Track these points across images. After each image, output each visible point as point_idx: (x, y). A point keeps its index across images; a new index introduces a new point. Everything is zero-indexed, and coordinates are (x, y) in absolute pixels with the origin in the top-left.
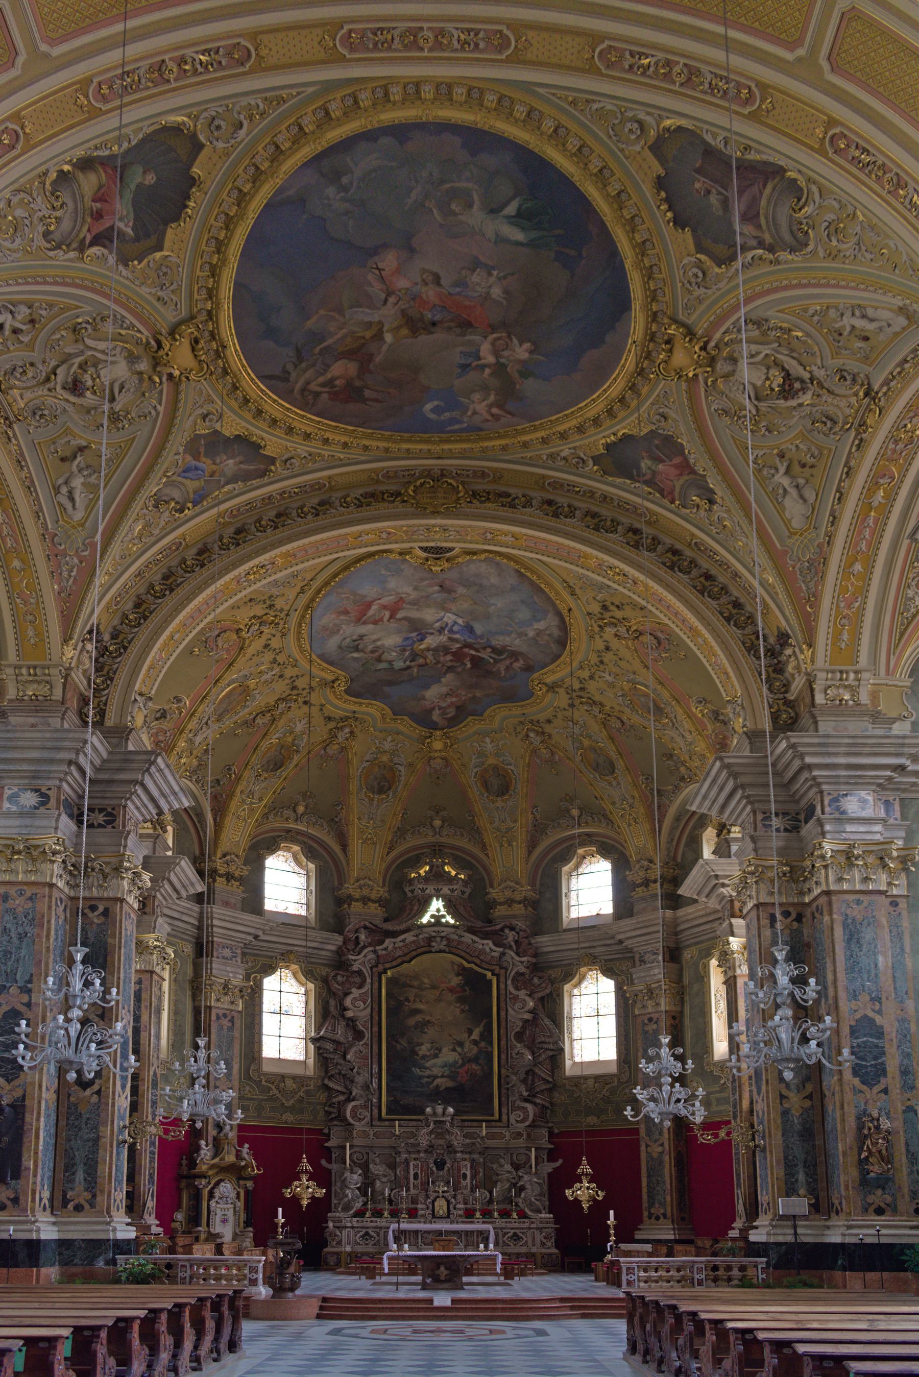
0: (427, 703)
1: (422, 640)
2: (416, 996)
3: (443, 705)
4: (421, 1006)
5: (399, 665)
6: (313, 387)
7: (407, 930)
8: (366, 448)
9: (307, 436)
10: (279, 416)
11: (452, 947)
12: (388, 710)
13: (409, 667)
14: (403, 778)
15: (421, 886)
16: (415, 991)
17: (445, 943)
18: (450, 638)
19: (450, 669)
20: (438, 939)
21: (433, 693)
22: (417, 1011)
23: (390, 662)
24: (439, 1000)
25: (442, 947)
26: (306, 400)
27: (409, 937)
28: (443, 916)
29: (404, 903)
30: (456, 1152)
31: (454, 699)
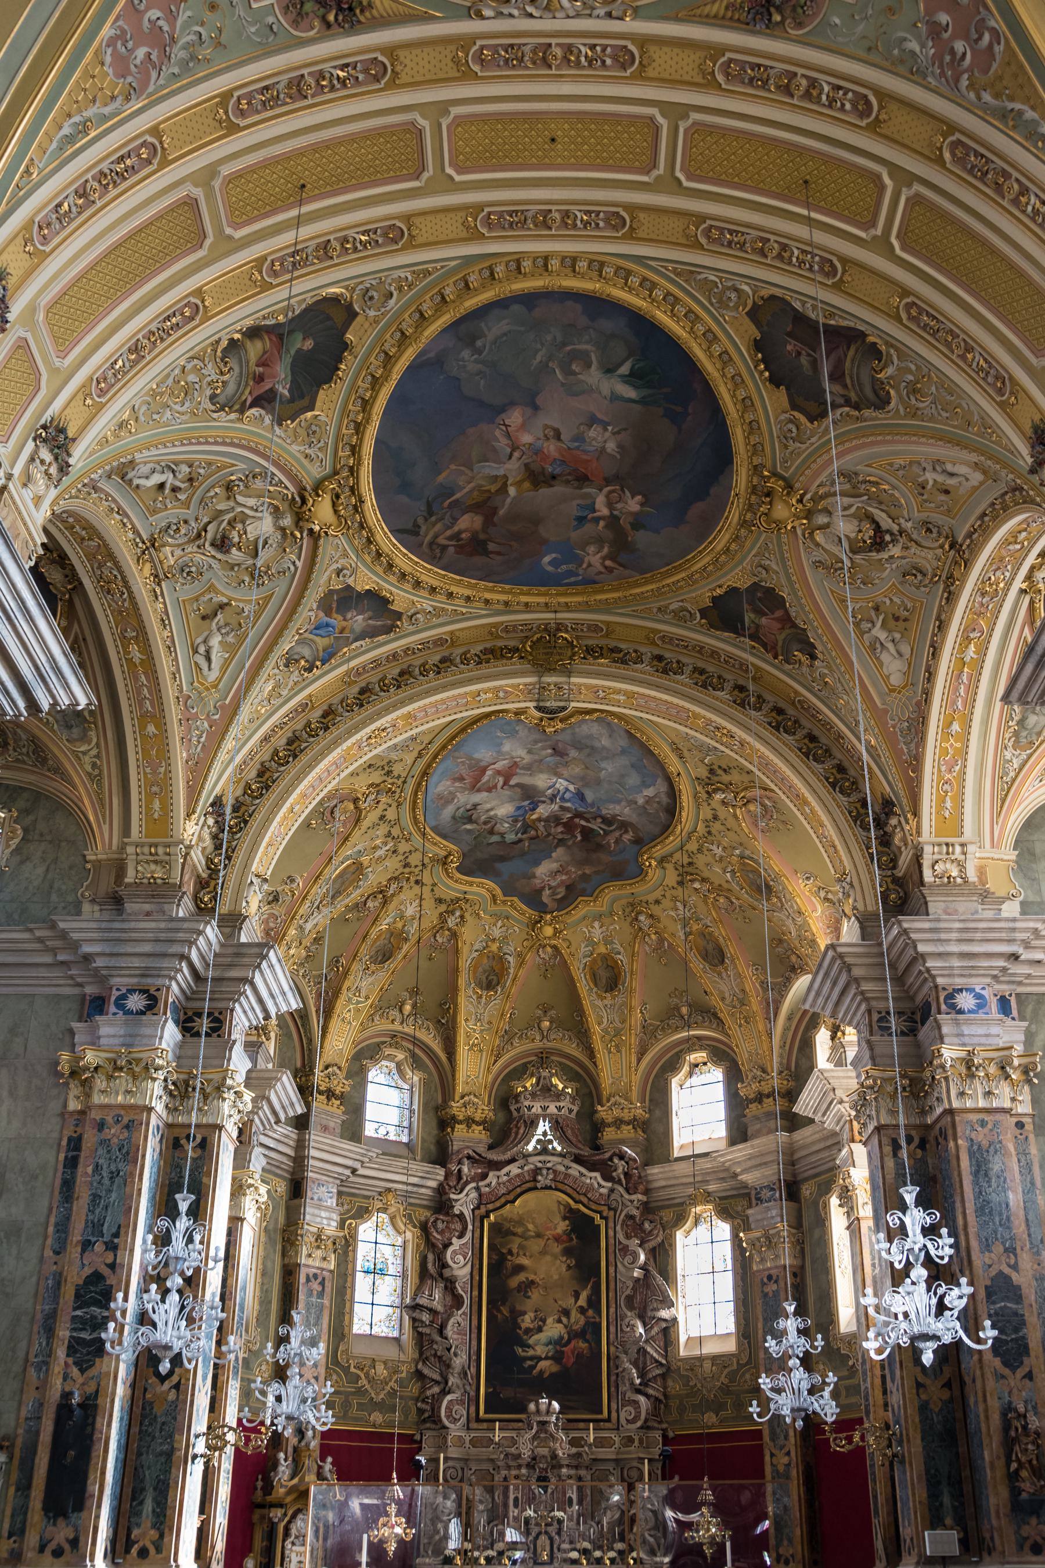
0: (537, 881)
1: (534, 809)
2: (521, 1247)
3: (553, 884)
4: (525, 1261)
5: (511, 837)
6: (441, 540)
7: (513, 1160)
8: (487, 602)
9: (433, 590)
10: (408, 569)
11: (559, 1184)
12: (498, 891)
13: (520, 841)
14: (512, 971)
15: (527, 1103)
16: (518, 1241)
17: (551, 1176)
18: (561, 807)
19: (561, 842)
20: (545, 1172)
21: (544, 870)
22: (520, 1268)
23: (502, 835)
24: (543, 1252)
25: (548, 1182)
26: (434, 554)
27: (514, 1169)
28: (550, 1142)
29: (508, 1125)
30: (561, 1466)
31: (564, 877)
